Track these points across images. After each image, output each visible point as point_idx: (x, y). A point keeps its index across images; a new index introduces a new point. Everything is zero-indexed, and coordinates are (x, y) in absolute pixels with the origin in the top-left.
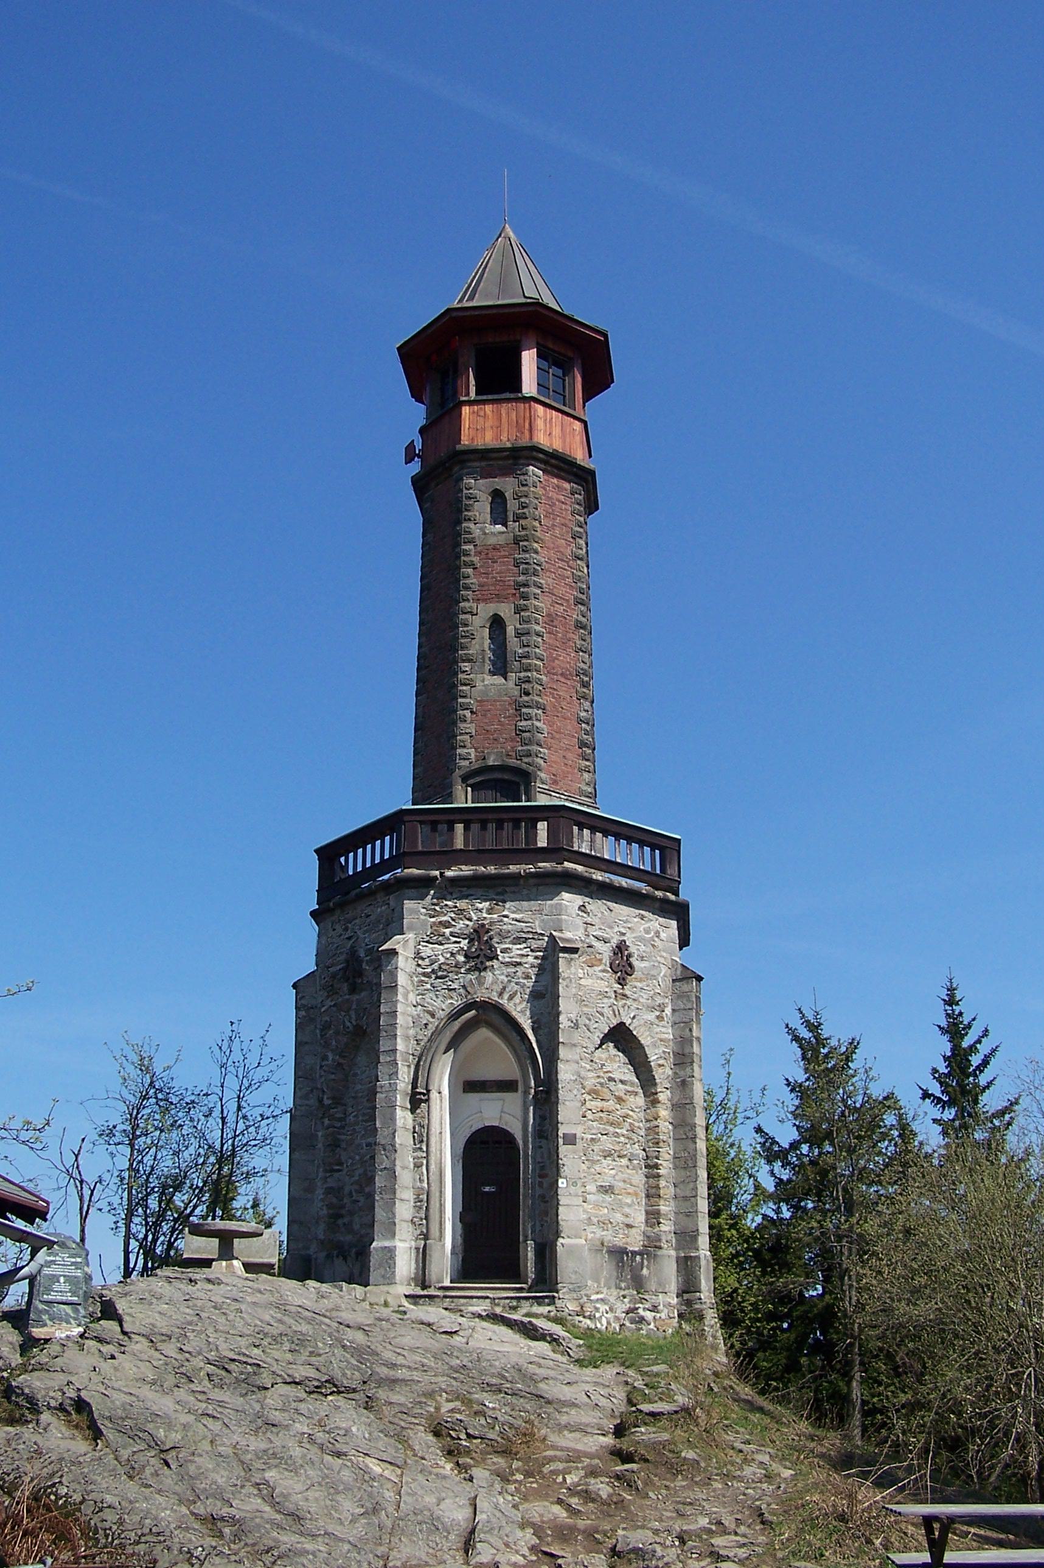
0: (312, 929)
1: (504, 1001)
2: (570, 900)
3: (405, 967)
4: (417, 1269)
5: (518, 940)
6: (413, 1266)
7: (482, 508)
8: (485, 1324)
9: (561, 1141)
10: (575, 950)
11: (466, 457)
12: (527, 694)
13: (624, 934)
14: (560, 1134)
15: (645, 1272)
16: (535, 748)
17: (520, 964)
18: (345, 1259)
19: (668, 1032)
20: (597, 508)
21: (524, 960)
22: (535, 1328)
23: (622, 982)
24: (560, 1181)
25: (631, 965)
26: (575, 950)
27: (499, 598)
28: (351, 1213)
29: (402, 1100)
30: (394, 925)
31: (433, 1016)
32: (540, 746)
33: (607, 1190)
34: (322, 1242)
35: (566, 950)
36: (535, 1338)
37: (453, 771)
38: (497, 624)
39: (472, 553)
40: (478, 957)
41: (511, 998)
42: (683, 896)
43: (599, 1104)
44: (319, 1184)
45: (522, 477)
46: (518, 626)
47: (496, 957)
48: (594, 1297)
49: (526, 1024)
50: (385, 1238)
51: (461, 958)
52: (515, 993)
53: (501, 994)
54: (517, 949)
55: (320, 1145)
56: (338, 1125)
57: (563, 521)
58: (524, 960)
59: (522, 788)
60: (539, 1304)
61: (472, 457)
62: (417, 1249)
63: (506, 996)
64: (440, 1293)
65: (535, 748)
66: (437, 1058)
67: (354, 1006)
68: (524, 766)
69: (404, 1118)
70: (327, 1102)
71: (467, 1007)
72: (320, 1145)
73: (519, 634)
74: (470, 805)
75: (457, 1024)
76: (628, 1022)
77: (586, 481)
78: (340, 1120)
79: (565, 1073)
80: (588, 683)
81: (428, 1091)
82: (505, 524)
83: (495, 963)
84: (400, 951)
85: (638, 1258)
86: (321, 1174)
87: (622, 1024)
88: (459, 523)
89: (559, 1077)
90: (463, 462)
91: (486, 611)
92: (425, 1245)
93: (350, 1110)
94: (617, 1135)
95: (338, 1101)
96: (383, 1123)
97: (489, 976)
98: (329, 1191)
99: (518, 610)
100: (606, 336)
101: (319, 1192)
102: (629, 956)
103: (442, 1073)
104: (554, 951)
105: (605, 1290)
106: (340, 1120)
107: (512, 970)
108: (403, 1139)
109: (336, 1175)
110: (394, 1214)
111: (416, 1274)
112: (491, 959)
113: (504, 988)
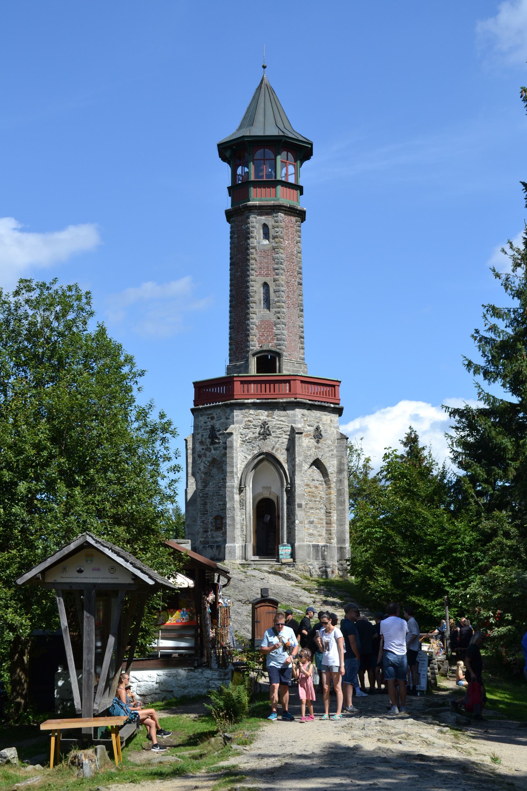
0: (191, 417)
1: (274, 452)
2: (298, 412)
3: (236, 441)
4: (242, 553)
6: (241, 552)
7: (257, 233)
8: (272, 575)
9: (296, 506)
10: (301, 433)
11: (252, 208)
12: (279, 318)
14: (296, 503)
15: (326, 553)
16: (283, 342)
17: (279, 437)
18: (212, 548)
19: (335, 462)
20: (305, 220)
22: (290, 576)
23: (318, 442)
24: (296, 521)
25: (321, 435)
26: (301, 433)
29: (236, 491)
30: (228, 421)
32: (284, 341)
33: (311, 522)
35: (298, 433)
36: (290, 580)
37: (248, 352)
38: (266, 285)
39: (255, 253)
40: (264, 434)
41: (277, 450)
42: (341, 405)
43: (309, 490)
44: (199, 519)
45: (275, 218)
46: (275, 288)
48: (309, 563)
49: (286, 466)
50: (231, 543)
52: (278, 449)
53: (273, 449)
55: (198, 504)
56: (206, 496)
59: (277, 359)
60: (289, 567)
61: (254, 208)
62: (242, 546)
63: (275, 450)
64: (252, 563)
65: (284, 347)
66: (248, 474)
68: (278, 350)
69: (237, 497)
71: (260, 454)
72: (198, 504)
73: (275, 292)
75: (256, 461)
76: (320, 457)
77: (302, 215)
79: (298, 481)
80: (302, 310)
81: (245, 487)
82: (269, 240)
83: (270, 437)
84: (234, 433)
85: (323, 548)
86: (199, 515)
87: (318, 459)
88: (249, 238)
89: (296, 482)
90: (250, 210)
91: (261, 280)
92: (245, 545)
94: (315, 501)
96: (229, 500)
99: (275, 280)
100: (312, 145)
102: (321, 431)
103: (250, 479)
104: (293, 433)
105: (312, 560)
107: (277, 439)
108: (237, 505)
109: (206, 515)
110: (234, 534)
111: (242, 555)
112: (269, 435)
113: (274, 447)
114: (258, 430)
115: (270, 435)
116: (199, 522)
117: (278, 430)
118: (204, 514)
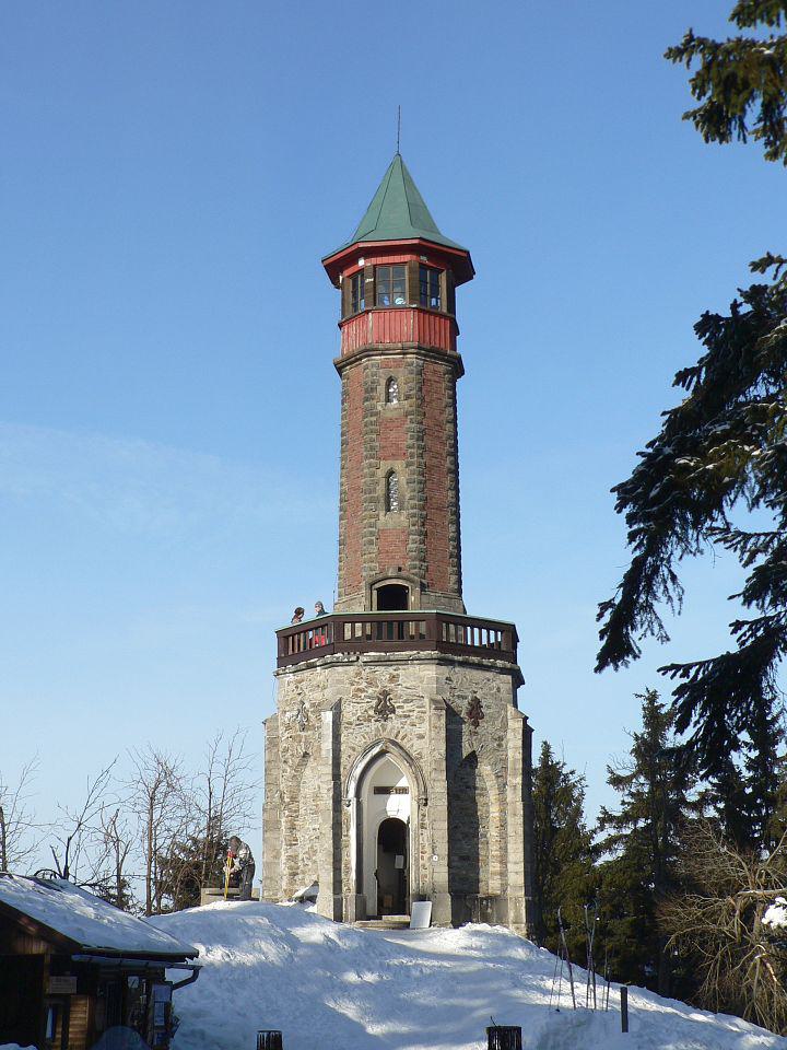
5: (406, 701)
13: (475, 692)
15: (489, 911)
21: (411, 714)
27: (394, 456)
28: (303, 873)
31: (354, 750)
34: (285, 891)
47: (393, 711)
51: (371, 712)
54: (407, 707)
57: (438, 396)
58: (411, 714)
63: (400, 736)
67: (303, 740)
70: (287, 800)
74: (375, 611)
78: (295, 811)
83: (393, 715)
93: (301, 805)
95: (294, 799)
97: (389, 724)
98: (290, 858)
100: (468, 253)
101: (283, 858)
106: (295, 811)
114: (374, 702)
115: (393, 711)
116: (283, 858)
117: (405, 705)
118: (291, 845)
